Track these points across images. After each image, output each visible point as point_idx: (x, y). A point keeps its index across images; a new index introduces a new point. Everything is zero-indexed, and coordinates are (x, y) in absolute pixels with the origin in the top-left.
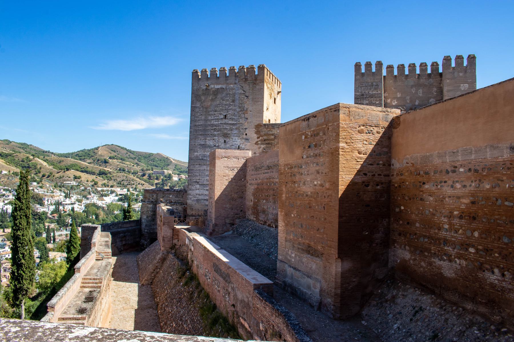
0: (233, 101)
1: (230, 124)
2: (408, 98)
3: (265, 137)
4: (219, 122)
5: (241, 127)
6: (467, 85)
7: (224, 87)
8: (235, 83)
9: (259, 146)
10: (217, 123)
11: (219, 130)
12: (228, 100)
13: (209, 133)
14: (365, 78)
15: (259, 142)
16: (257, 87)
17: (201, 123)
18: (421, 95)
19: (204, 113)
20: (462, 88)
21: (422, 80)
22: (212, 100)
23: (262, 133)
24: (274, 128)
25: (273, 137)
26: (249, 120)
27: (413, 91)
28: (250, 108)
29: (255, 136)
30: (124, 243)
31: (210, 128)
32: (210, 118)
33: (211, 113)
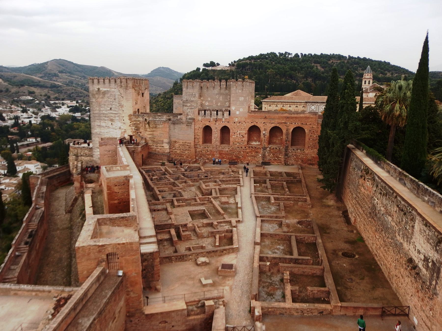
0: (115, 99)
1: (114, 113)
2: (214, 101)
3: (135, 122)
4: (108, 112)
5: (120, 116)
6: (243, 98)
7: (109, 90)
8: (115, 88)
9: (131, 127)
10: (106, 112)
11: (108, 117)
12: (111, 99)
13: (102, 118)
14: (188, 90)
15: (131, 125)
16: (128, 91)
17: (97, 112)
18: (221, 100)
19: (98, 106)
20: (241, 100)
21: (222, 91)
22: (102, 98)
23: (133, 120)
24: (139, 117)
25: (139, 122)
26: (125, 112)
27: (217, 96)
28: (125, 105)
29: (129, 121)
30: (59, 181)
31: (102, 115)
32: (102, 109)
33: (102, 106)
